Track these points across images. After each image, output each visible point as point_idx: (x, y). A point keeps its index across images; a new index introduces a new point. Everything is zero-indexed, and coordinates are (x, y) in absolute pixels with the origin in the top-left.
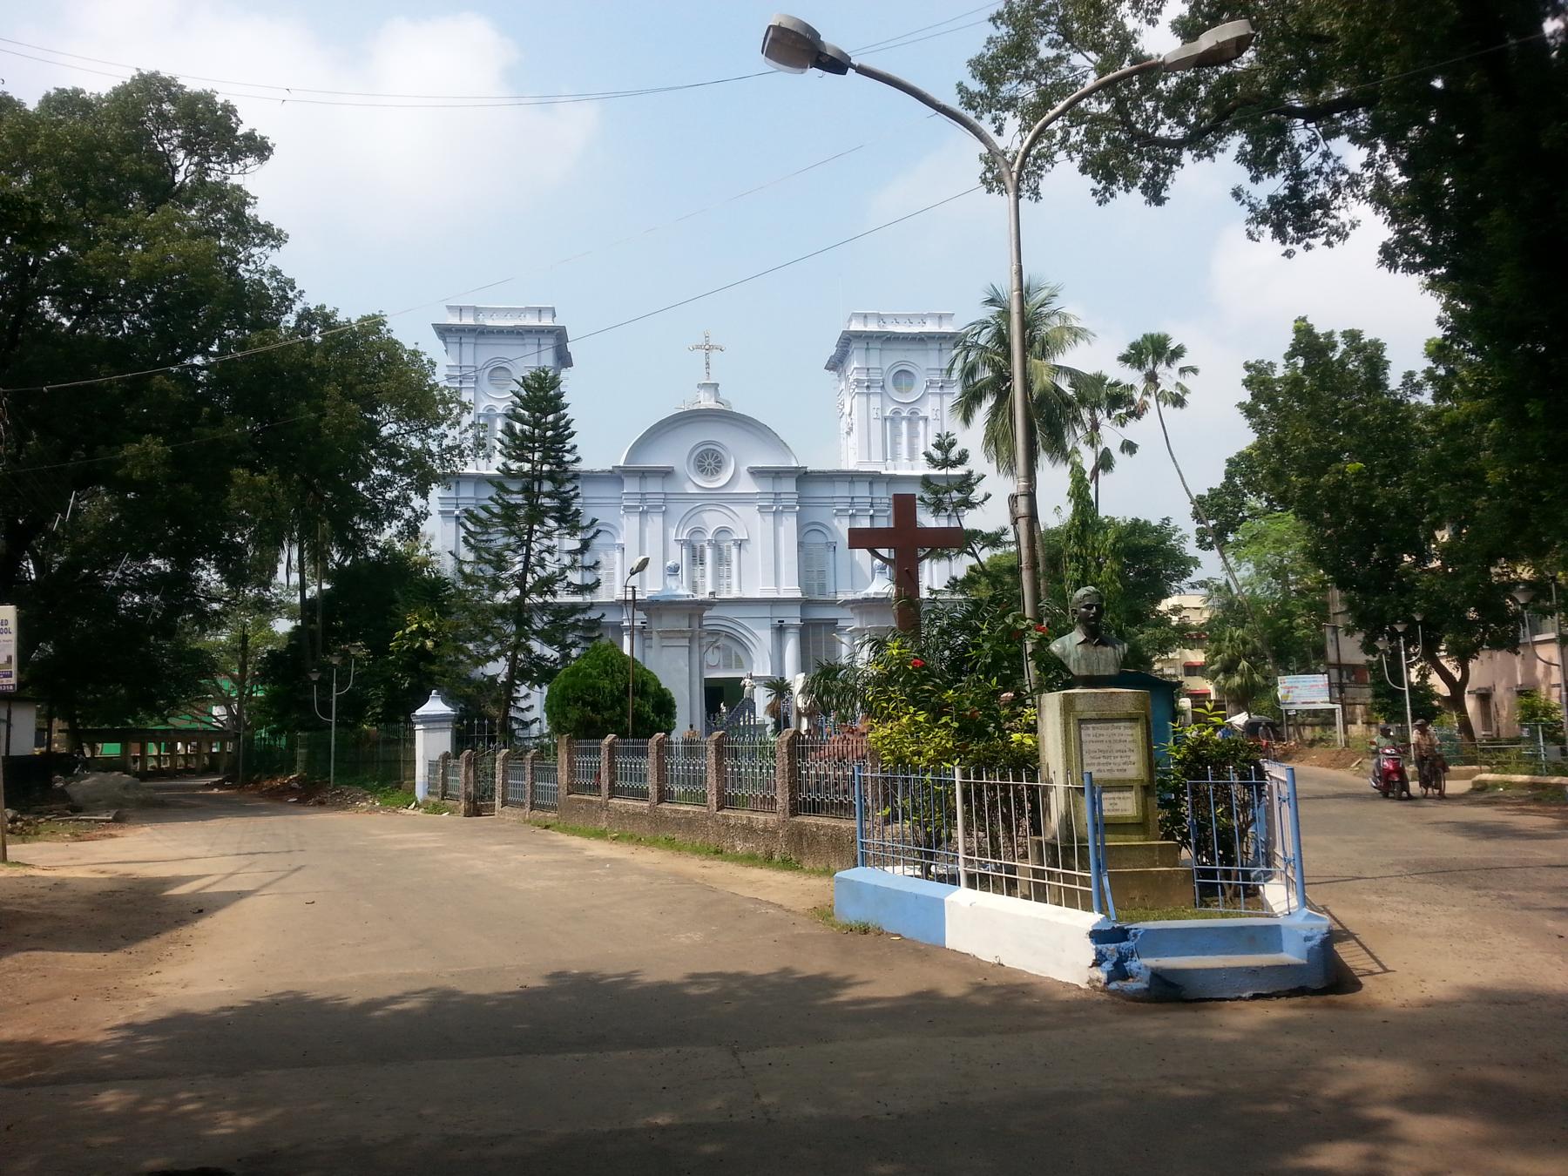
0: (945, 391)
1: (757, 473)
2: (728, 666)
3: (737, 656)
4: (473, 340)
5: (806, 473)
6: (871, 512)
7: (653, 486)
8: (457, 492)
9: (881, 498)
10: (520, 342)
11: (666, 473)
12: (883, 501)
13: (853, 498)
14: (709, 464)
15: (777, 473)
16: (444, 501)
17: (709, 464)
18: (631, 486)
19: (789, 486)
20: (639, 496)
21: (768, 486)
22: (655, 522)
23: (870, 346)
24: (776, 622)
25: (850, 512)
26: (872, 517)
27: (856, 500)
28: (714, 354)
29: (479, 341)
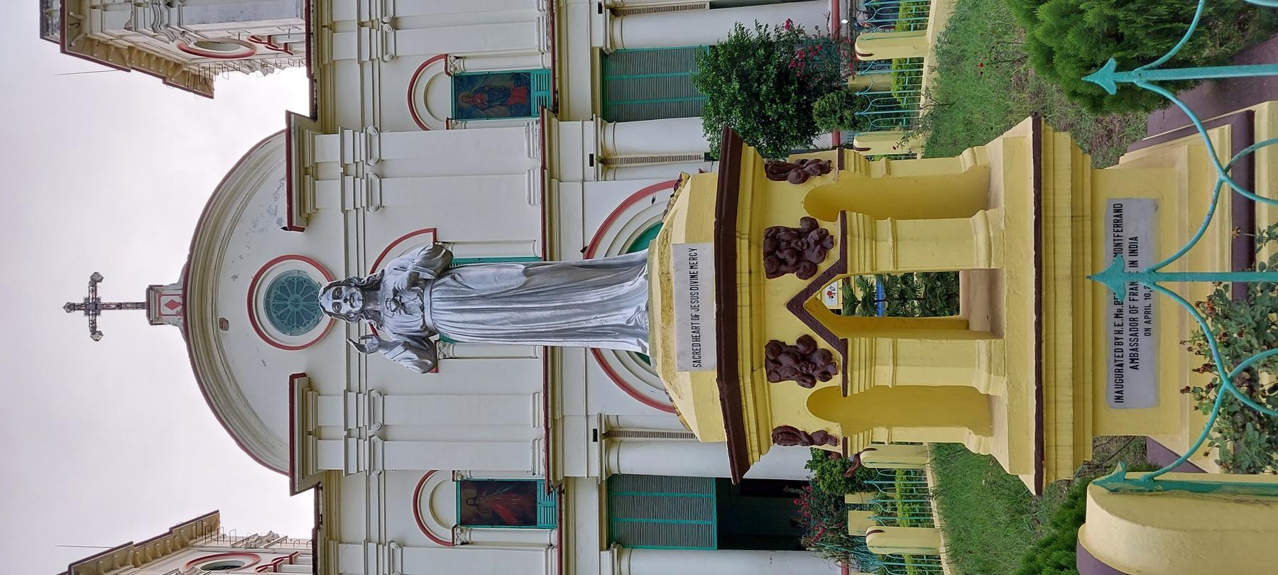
5: (314, 116)
7: (331, 413)
13: (361, 25)
14: (296, 305)
15: (303, 171)
17: (296, 305)
18: (331, 456)
19: (328, 148)
20: (352, 441)
21: (328, 193)
22: (395, 412)
24: (591, 171)
25: (386, 27)
27: (365, 18)
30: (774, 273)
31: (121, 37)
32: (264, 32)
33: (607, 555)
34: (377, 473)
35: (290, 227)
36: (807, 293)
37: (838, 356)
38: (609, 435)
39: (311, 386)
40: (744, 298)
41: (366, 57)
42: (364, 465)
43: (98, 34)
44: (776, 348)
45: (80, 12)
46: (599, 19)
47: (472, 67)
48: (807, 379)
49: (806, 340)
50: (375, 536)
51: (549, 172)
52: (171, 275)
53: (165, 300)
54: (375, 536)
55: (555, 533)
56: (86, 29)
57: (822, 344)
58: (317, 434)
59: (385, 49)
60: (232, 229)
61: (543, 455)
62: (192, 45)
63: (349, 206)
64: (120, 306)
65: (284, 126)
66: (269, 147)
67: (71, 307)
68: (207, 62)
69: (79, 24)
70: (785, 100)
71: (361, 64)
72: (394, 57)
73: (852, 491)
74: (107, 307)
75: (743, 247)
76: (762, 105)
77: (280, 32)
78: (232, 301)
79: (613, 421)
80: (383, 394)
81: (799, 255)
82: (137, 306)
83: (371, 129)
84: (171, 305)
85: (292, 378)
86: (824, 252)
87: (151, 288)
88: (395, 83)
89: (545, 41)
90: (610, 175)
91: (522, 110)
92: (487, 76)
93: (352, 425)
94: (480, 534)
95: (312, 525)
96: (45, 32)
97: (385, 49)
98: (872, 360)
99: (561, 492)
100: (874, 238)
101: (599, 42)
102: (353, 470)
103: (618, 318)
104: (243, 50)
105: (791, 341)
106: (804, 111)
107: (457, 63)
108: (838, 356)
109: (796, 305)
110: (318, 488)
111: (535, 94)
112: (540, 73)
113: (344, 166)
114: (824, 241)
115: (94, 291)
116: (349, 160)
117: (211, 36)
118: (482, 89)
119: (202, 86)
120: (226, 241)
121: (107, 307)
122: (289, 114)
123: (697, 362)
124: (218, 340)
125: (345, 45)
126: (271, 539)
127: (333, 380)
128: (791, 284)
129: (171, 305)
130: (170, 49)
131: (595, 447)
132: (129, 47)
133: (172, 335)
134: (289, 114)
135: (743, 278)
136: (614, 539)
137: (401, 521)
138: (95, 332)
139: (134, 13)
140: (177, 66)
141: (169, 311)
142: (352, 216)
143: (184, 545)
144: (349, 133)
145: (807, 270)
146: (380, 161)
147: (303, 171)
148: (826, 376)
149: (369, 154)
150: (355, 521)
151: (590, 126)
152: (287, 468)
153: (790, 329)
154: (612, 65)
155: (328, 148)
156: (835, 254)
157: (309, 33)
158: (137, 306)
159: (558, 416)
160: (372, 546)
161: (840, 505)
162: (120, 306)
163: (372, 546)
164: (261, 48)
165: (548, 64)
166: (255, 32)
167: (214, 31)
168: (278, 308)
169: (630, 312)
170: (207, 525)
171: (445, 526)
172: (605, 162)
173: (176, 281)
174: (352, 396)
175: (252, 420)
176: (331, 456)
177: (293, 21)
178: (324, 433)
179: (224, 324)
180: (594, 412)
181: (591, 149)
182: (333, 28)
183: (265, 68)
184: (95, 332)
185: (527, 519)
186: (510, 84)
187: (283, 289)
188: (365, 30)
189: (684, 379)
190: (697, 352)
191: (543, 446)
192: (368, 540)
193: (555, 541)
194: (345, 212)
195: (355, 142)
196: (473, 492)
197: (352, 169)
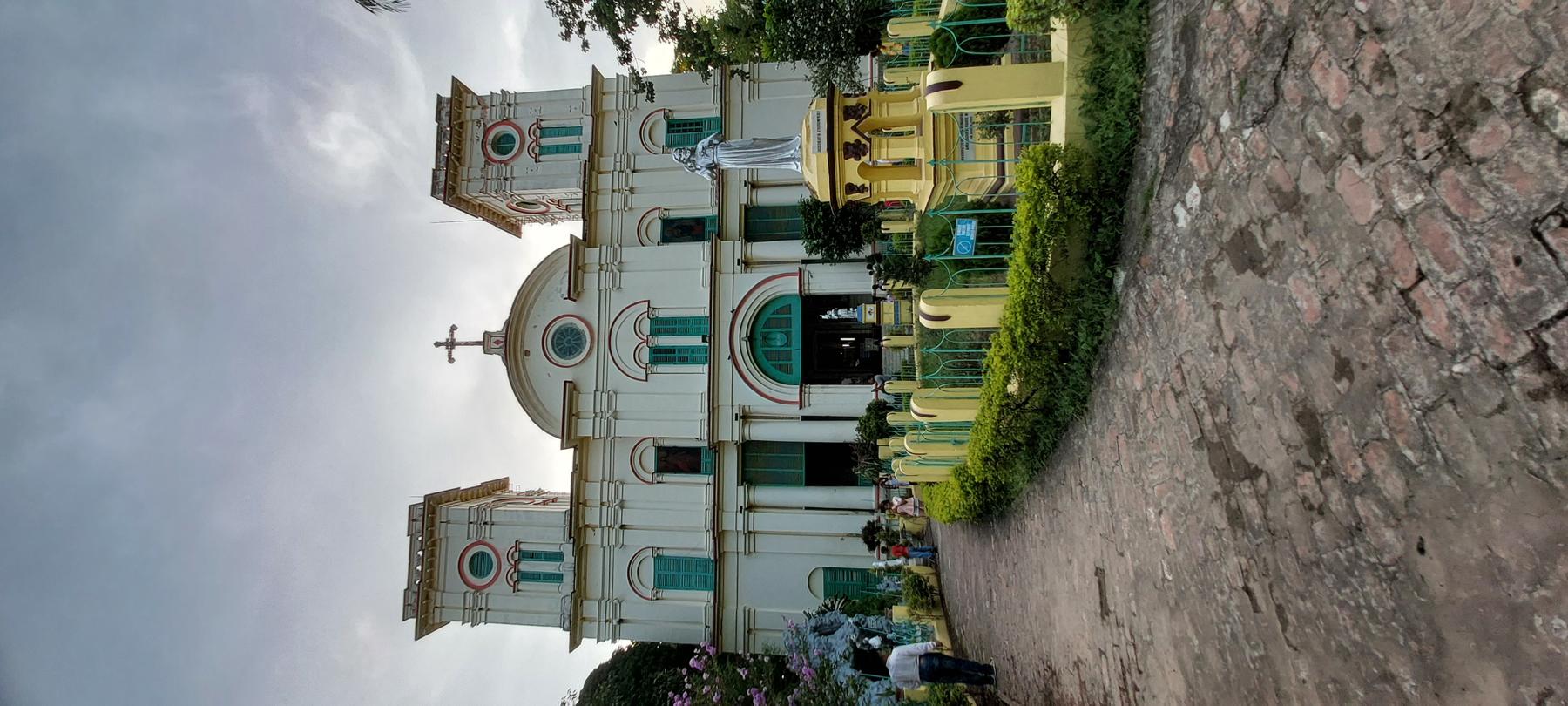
0: (512, 102)
1: (575, 292)
2: (788, 323)
3: (777, 312)
4: (439, 594)
6: (628, 171)
7: (586, 403)
8: (592, 621)
9: (616, 162)
10: (444, 541)
11: (571, 390)
12: (618, 159)
13: (613, 191)
14: (569, 342)
15: (578, 268)
16: (602, 637)
18: (585, 428)
19: (592, 255)
20: (598, 420)
21: (591, 281)
22: (622, 404)
23: (465, 178)
24: (738, 268)
25: (627, 193)
26: (634, 171)
27: (616, 187)
28: (458, 337)
29: (441, 588)
30: (846, 119)
31: (476, 197)
32: (556, 197)
33: (741, 488)
34: (610, 439)
35: (569, 298)
36: (857, 124)
37: (868, 144)
38: (745, 417)
39: (575, 388)
40: (836, 125)
41: (615, 209)
42: (604, 434)
43: (465, 195)
44: (847, 144)
45: (455, 182)
46: (745, 190)
47: (673, 215)
48: (858, 158)
49: (858, 141)
50: (607, 478)
51: (715, 268)
52: (497, 326)
53: (493, 339)
54: (607, 478)
55: (712, 477)
56: (458, 192)
57: (863, 141)
58: (577, 416)
59: (626, 204)
60: (535, 300)
61: (706, 428)
62: (514, 205)
63: (602, 288)
64: (466, 344)
65: (569, 242)
66: (558, 255)
67: (438, 344)
68: (521, 217)
69: (454, 189)
70: (846, 224)
71: (612, 211)
72: (631, 209)
73: (881, 438)
74: (460, 344)
75: (836, 107)
76: (834, 226)
77: (564, 196)
78: (533, 341)
79: (747, 409)
80: (616, 393)
81: (855, 112)
82: (478, 343)
83: (616, 246)
84: (497, 342)
85: (566, 382)
86: (863, 111)
87: (486, 333)
88: (631, 223)
89: (714, 200)
90: (749, 270)
91: (699, 237)
92: (682, 219)
93: (598, 411)
94: (667, 477)
95: (571, 470)
96: (434, 193)
97: (626, 204)
98: (880, 147)
99: (716, 452)
100: (880, 106)
101: (744, 201)
102: (597, 436)
103: (787, 155)
104: (543, 208)
105: (852, 142)
106: (856, 230)
107: (666, 213)
108: (868, 144)
109: (854, 128)
110: (575, 448)
111: (707, 229)
112: (712, 219)
113: (601, 265)
114: (864, 108)
115: (452, 335)
116: (603, 262)
117: (527, 198)
118: (677, 227)
119: (515, 230)
120: (531, 307)
121: (460, 344)
122: (571, 236)
123: (819, 150)
124: (523, 362)
125: (604, 202)
126: (540, 492)
127: (588, 384)
128: (853, 122)
129: (497, 342)
130: (500, 205)
131: (736, 423)
132: (480, 205)
133: (497, 360)
134: (571, 236)
135: (836, 118)
136: (747, 479)
137: (622, 469)
138: (451, 360)
139: (486, 184)
140: (504, 218)
141: (496, 346)
142: (603, 292)
143: (489, 494)
144: (604, 247)
145: (860, 118)
146: (621, 263)
147: (578, 268)
148: (864, 154)
149: (615, 260)
150: (596, 469)
151: (738, 244)
152: (560, 435)
153: (852, 137)
154: (750, 213)
155: (592, 255)
156: (867, 111)
157: (584, 195)
158: (478, 343)
159: (715, 406)
160: (605, 483)
161: (876, 448)
162: (466, 344)
163: (605, 483)
164: (553, 208)
165: (716, 213)
166: (551, 197)
167: (529, 195)
168: (558, 344)
169: (792, 151)
170: (502, 484)
171: (649, 473)
172: (747, 264)
173: (500, 329)
174: (598, 394)
175: (540, 408)
176: (585, 428)
177: (574, 190)
178: (582, 415)
179: (527, 353)
180: (736, 404)
181: (738, 256)
182: (597, 192)
183: (553, 221)
184: (451, 360)
185: (695, 469)
186: (693, 224)
187: (562, 334)
188: (615, 194)
189: (814, 158)
190: (819, 147)
191: (706, 422)
192: (603, 480)
193: (711, 481)
194: (600, 291)
195: (607, 253)
196: (664, 454)
197: (605, 267)
